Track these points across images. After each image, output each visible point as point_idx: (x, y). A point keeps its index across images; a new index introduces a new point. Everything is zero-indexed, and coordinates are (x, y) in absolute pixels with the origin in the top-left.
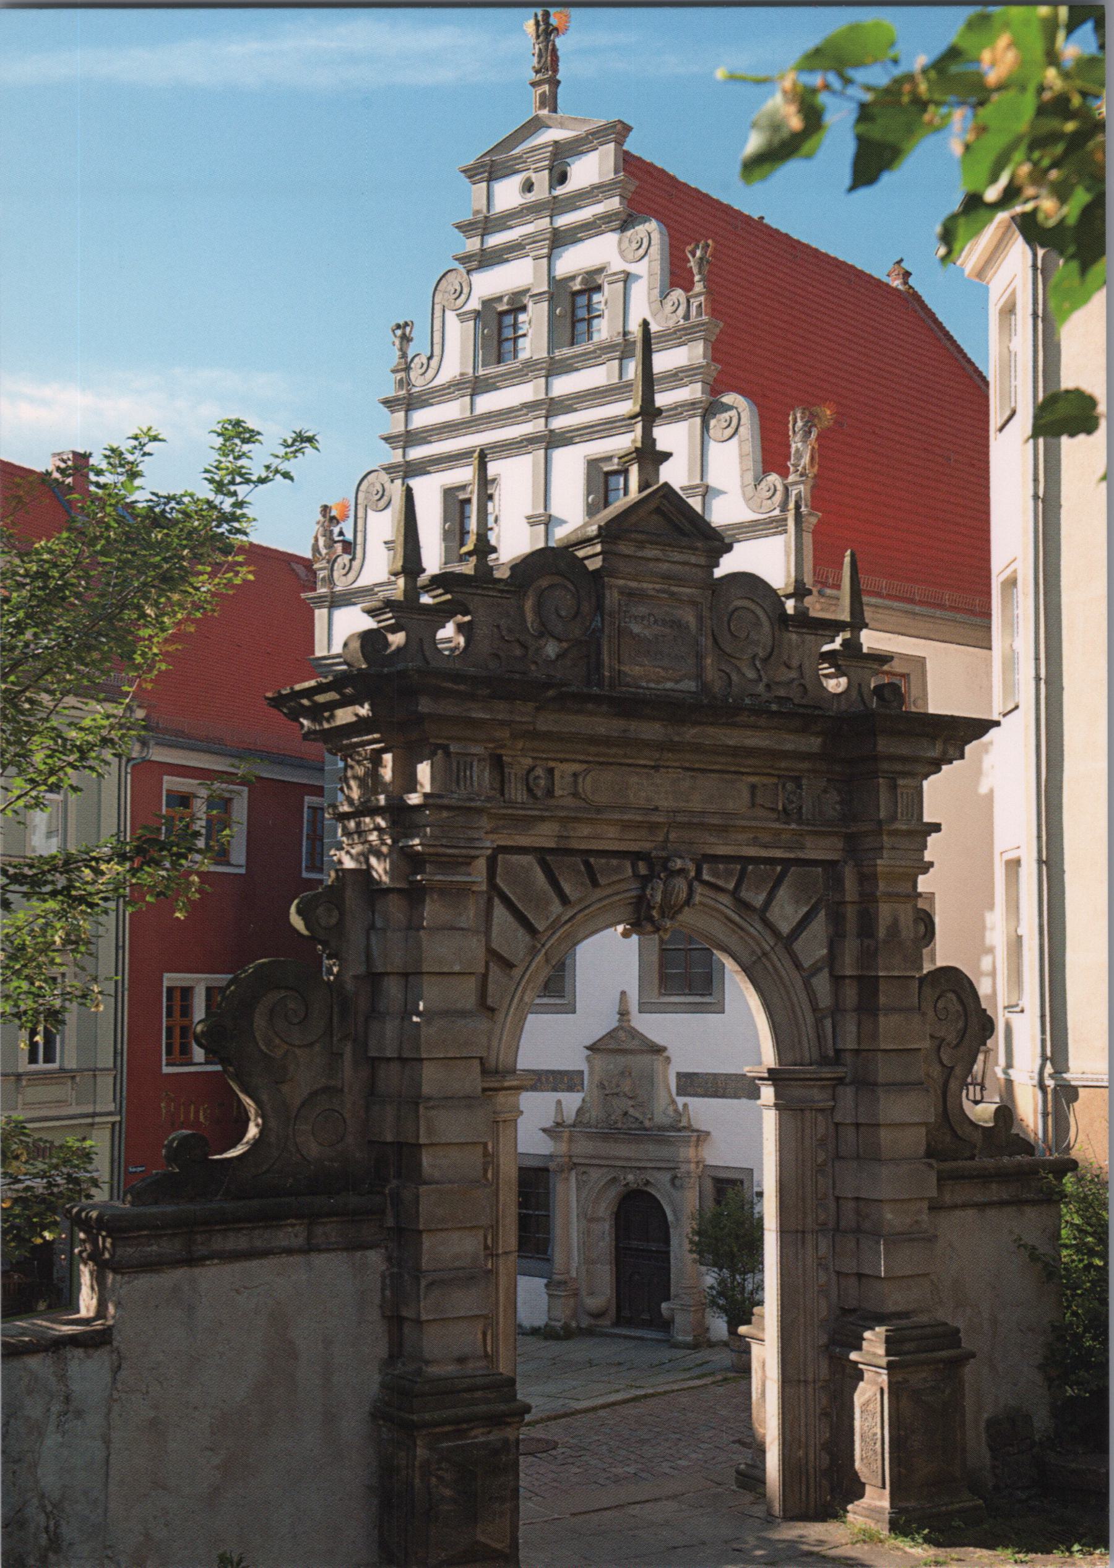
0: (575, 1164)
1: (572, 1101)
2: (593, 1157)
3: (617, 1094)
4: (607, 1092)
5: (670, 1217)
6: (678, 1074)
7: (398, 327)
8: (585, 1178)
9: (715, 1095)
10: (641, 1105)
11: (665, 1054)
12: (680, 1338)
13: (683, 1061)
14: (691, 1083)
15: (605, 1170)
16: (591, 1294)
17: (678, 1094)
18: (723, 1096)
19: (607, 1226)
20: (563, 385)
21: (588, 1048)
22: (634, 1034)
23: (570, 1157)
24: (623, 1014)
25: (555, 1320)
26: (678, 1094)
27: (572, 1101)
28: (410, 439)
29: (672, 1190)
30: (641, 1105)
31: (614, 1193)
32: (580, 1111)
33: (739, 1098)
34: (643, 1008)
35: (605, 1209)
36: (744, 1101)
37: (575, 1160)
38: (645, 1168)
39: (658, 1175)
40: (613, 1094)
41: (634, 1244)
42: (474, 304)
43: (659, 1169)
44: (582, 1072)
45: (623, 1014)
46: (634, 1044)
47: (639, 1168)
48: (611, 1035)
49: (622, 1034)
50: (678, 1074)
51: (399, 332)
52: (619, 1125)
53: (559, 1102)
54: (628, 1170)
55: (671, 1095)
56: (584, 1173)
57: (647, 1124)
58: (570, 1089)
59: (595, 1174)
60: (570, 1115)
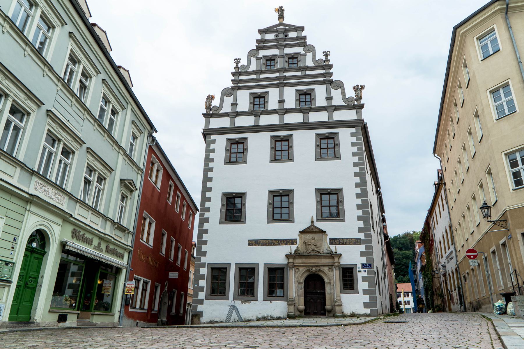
0: (295, 266)
1: (294, 248)
3: (310, 245)
4: (307, 244)
5: (326, 280)
7: (236, 59)
8: (297, 270)
9: (343, 244)
10: (318, 247)
11: (326, 233)
12: (338, 314)
13: (331, 235)
14: (334, 241)
15: (304, 268)
16: (299, 305)
18: (346, 244)
19: (303, 285)
20: (286, 74)
21: (300, 232)
22: (316, 228)
24: (312, 222)
27: (294, 248)
28: (240, 81)
29: (328, 272)
30: (318, 247)
31: (306, 275)
32: (295, 251)
33: (351, 245)
34: (318, 220)
35: (302, 280)
37: (295, 265)
38: (319, 266)
39: (323, 268)
40: (309, 245)
41: (312, 290)
42: (260, 56)
43: (324, 266)
44: (296, 239)
45: (312, 222)
46: (317, 230)
47: (317, 266)
48: (309, 228)
51: (236, 60)
52: (311, 253)
53: (291, 247)
54: (313, 267)
58: (292, 244)
59: (301, 269)
60: (293, 252)
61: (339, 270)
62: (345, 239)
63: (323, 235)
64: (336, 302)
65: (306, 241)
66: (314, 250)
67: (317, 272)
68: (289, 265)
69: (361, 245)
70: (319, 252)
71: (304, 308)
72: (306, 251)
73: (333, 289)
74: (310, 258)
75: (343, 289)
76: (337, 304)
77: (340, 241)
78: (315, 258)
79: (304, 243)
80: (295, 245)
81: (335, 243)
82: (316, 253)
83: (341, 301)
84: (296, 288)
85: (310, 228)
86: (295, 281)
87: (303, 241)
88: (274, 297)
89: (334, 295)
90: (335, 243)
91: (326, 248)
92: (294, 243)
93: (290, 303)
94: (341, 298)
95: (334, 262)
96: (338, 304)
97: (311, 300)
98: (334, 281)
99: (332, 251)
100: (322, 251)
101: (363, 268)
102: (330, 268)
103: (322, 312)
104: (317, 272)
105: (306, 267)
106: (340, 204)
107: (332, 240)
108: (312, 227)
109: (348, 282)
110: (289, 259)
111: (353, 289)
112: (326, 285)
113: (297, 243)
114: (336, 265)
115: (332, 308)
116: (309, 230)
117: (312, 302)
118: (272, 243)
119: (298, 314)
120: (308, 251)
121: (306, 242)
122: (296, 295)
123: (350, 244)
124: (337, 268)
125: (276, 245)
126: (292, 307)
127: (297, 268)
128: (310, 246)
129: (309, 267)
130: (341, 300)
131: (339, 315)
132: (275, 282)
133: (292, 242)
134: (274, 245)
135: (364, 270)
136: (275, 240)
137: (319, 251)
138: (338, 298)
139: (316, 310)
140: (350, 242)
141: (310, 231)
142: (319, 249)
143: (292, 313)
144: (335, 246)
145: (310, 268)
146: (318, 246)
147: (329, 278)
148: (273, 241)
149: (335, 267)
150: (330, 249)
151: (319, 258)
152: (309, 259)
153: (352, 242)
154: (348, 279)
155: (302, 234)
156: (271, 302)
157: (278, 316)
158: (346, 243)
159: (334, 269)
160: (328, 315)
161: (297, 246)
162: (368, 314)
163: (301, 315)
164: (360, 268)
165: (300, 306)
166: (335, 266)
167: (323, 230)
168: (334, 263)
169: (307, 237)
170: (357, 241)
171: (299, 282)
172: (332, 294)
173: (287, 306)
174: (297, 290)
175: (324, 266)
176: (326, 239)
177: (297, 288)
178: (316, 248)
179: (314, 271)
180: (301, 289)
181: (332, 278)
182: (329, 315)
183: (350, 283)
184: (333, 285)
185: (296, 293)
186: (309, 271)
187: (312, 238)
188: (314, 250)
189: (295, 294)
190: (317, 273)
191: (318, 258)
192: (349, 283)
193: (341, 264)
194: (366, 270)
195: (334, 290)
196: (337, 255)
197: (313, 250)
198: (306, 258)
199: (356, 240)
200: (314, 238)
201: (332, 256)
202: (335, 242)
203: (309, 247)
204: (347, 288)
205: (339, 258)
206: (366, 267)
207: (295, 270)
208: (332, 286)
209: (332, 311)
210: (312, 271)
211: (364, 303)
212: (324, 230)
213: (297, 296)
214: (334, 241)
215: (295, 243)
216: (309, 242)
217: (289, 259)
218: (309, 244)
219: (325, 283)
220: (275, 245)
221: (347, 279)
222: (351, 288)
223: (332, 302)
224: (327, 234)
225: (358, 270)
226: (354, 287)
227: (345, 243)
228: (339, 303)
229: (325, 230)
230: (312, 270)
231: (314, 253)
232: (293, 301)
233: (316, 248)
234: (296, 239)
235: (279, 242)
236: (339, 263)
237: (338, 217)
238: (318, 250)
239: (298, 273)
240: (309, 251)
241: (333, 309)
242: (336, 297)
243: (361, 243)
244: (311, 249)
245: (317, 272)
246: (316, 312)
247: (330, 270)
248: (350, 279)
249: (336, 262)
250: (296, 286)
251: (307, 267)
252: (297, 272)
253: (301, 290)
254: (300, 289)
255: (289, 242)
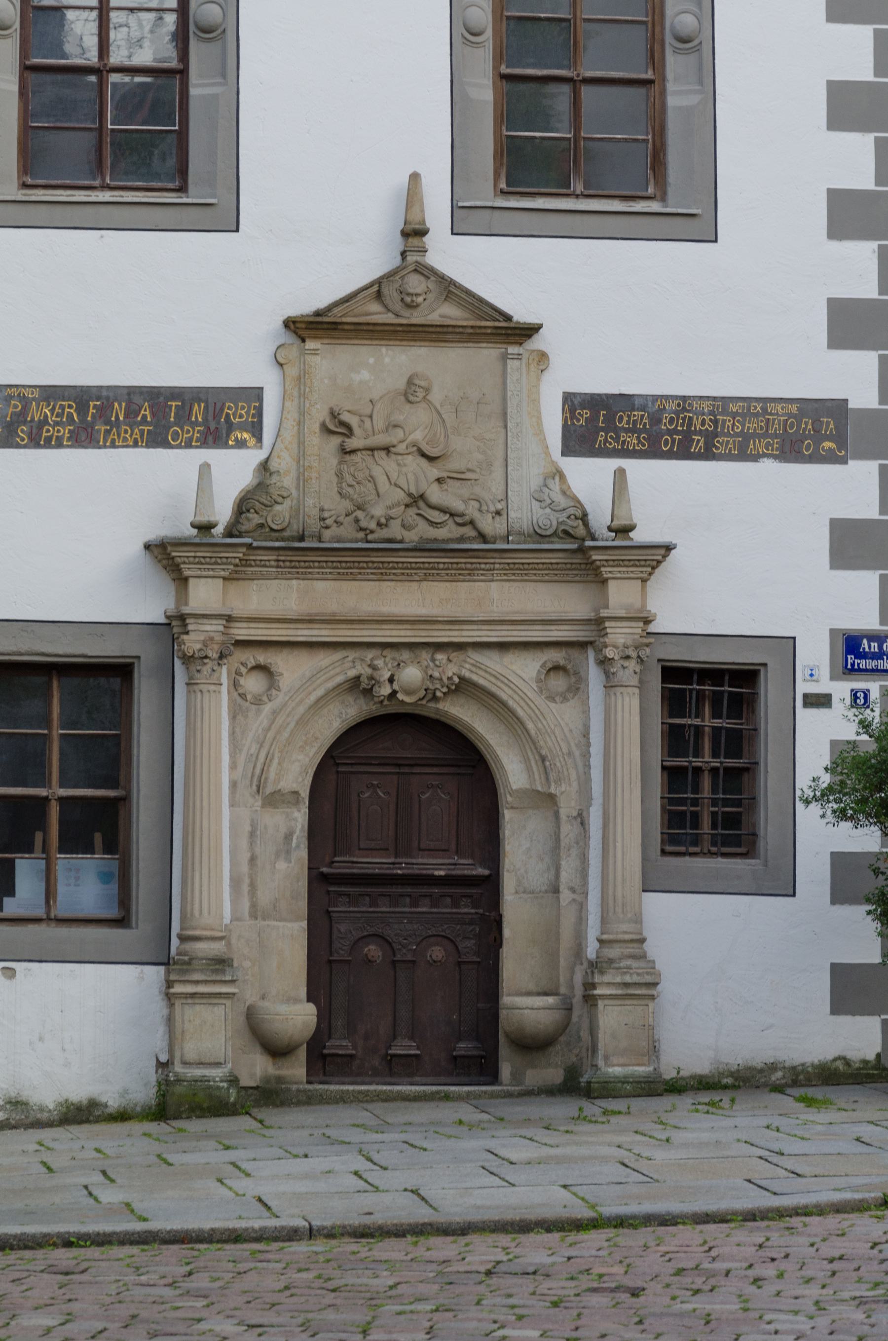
2: (309, 621)
3: (387, 449)
4: (353, 443)
6: (569, 399)
8: (253, 684)
9: (684, 452)
10: (459, 478)
11: (537, 343)
15: (324, 659)
17: (567, 451)
18: (708, 454)
19: (300, 817)
21: (291, 324)
23: (229, 619)
25: (201, 1064)
26: (567, 451)
29: (540, 701)
30: (459, 478)
32: (243, 506)
33: (755, 458)
36: (768, 466)
37: (242, 632)
38: (460, 647)
39: (492, 661)
40: (372, 450)
43: (503, 647)
44: (257, 394)
47: (439, 647)
49: (416, 283)
50: (569, 399)
52: (395, 530)
53: (205, 469)
54: (406, 655)
55: (547, 454)
56: (259, 668)
57: (488, 525)
61: (642, 685)
62: (706, 407)
63: (504, 358)
64: (595, 966)
65: (346, 417)
66: (422, 497)
67: (440, 706)
68: (192, 642)
69: (843, 461)
70: (472, 523)
71: (315, 1019)
72: (347, 505)
73: (574, 852)
74: (383, 574)
75: (664, 852)
76: (609, 984)
77: (656, 420)
78: (429, 574)
79: (326, 430)
80: (241, 444)
81: (617, 440)
82: (441, 533)
83: (643, 957)
84: (244, 843)
85: (390, 291)
86: (234, 785)
87: (319, 414)
88: (31, 927)
89: (582, 907)
90: (617, 440)
91: (535, 482)
92: (230, 427)
93: (196, 977)
94: (645, 934)
95: (604, 613)
96: (626, 985)
97: (373, 950)
98: (588, 780)
99: (584, 518)
100: (498, 513)
101: (851, 671)
102: (556, 668)
103: (464, 1047)
104: (435, 698)
105: (338, 655)
106: (674, 63)
107: (587, 413)
108: (416, 283)
109: (706, 791)
110: (181, 581)
111: (750, 853)
112: (508, 816)
113: (257, 430)
114: (621, 641)
115: (556, 1016)
116: (375, 313)
117: (369, 962)
118: (21, 417)
119: (259, 1072)
120: (359, 508)
121: (353, 421)
122: (246, 904)
123: (744, 455)
124: (628, 673)
125: (59, 445)
126: (219, 1011)
127: (259, 668)
128: (389, 464)
129: (370, 654)
130: (652, 948)
131: (624, 1080)
132: (42, 792)
133: (216, 417)
134: (36, 441)
135: (854, 695)
136: (50, 393)
137: (471, 510)
138: (622, 929)
139: (412, 1038)
140: (746, 437)
141: (389, 318)
142: (464, 490)
143: (218, 1064)
144: (620, 475)
145: (379, 663)
146: (455, 464)
147: (543, 759)
148: (23, 399)
149: (604, 662)
150: (566, 492)
151: (469, 574)
152: (368, 587)
153: (766, 435)
154: (707, 760)
155: (310, 344)
156: (10, 973)
157: (78, 1094)
158: (710, 437)
159: (594, 675)
160: (517, 1077)
161: (257, 456)
162: (865, 1062)
163: (280, 1079)
164: (825, 671)
165: (284, 1009)
166: (609, 653)
167: (508, 318)
168: (598, 623)
169: (356, 378)
170: (807, 425)
171: (269, 790)
172: (566, 896)
173: (159, 1007)
174: (253, 860)
175: (503, 647)
176: (535, 402)
177: (252, 844)
178: (439, 480)
179: (408, 693)
180: (286, 852)
181: (570, 754)
182: (534, 1077)
183: (726, 802)
184: (580, 815)
185: (245, 888)
186: (368, 692)
187: (401, 384)
188: (422, 497)
189: (234, 902)
190: (430, 709)
191: (456, 575)
192: (714, 802)
193: (653, 628)
194: (874, 687)
195: (584, 859)
196: (634, 555)
197: (417, 500)
198: (341, 577)
199: (799, 417)
200: (427, 390)
201: (582, 550)
202: (611, 425)
203: (377, 472)
204: (696, 841)
205: (644, 581)
206: (871, 664)
207: (235, 685)
208: (568, 831)
209: (562, 1039)
210: (394, 693)
211: (837, 970)
212: (522, 315)
213: (254, 915)
214: (610, 419)
215: (243, 428)
216: (379, 423)
217: (181, 581)
218: (370, 442)
219: (506, 799)
220: (48, 444)
221: (697, 762)
222: (727, 841)
223: (563, 963)
224: (543, 356)
225: (803, 687)
226: (755, 835)
227: (699, 444)
228: (628, 979)
229: (539, 322)
230: (391, 680)
231: (422, 531)
232: (221, 963)
233: (439, 480)
234: (257, 394)
235: (82, 408)
236: (647, 621)
237: (651, 190)
238: (457, 505)
239: (267, 708)
240: (378, 511)
241: (565, 1026)
242: (604, 921)
243: (842, 443)
244: (399, 496)
245: (435, 698)
246: (403, 1047)
247: (558, 683)
248: (731, 762)
249: (622, 613)
250: (248, 828)
251: (352, 654)
252: (258, 702)
253: (282, 865)
254: (277, 855)
255: (184, 416)
